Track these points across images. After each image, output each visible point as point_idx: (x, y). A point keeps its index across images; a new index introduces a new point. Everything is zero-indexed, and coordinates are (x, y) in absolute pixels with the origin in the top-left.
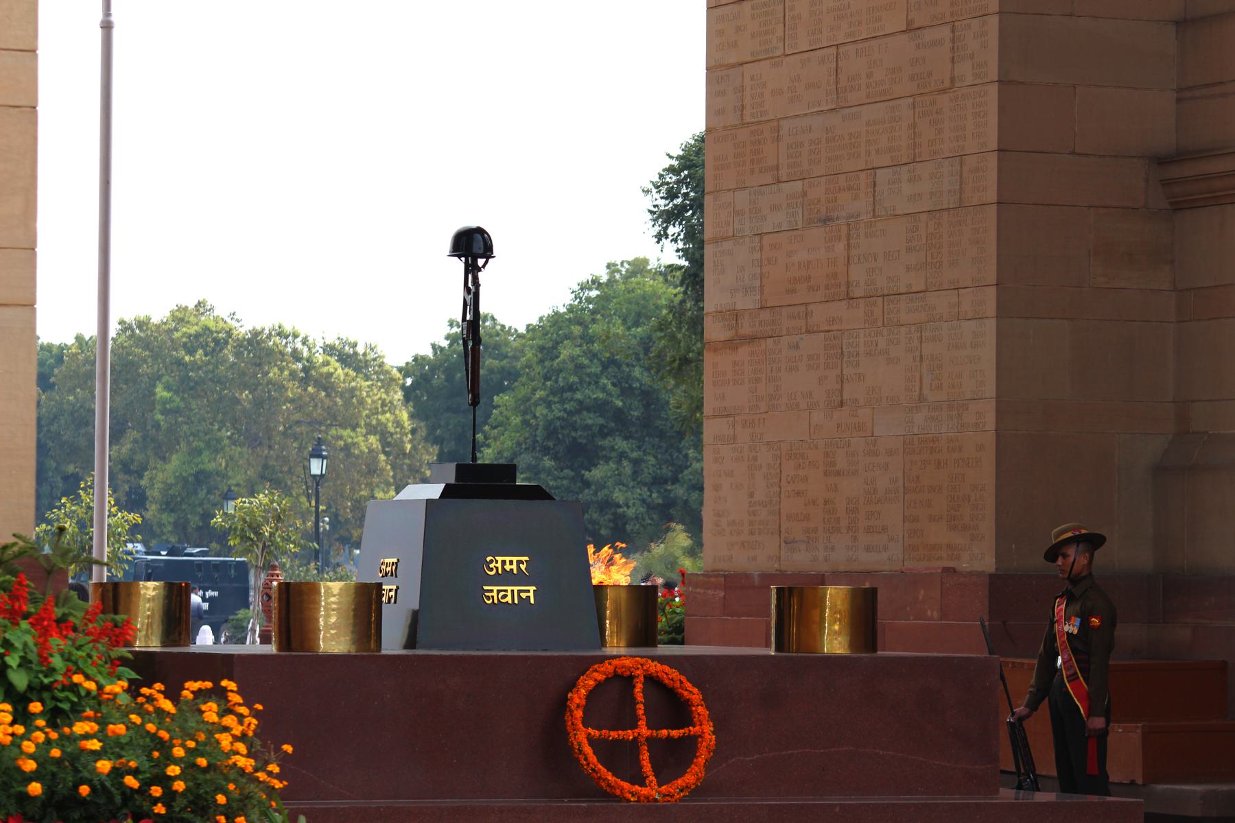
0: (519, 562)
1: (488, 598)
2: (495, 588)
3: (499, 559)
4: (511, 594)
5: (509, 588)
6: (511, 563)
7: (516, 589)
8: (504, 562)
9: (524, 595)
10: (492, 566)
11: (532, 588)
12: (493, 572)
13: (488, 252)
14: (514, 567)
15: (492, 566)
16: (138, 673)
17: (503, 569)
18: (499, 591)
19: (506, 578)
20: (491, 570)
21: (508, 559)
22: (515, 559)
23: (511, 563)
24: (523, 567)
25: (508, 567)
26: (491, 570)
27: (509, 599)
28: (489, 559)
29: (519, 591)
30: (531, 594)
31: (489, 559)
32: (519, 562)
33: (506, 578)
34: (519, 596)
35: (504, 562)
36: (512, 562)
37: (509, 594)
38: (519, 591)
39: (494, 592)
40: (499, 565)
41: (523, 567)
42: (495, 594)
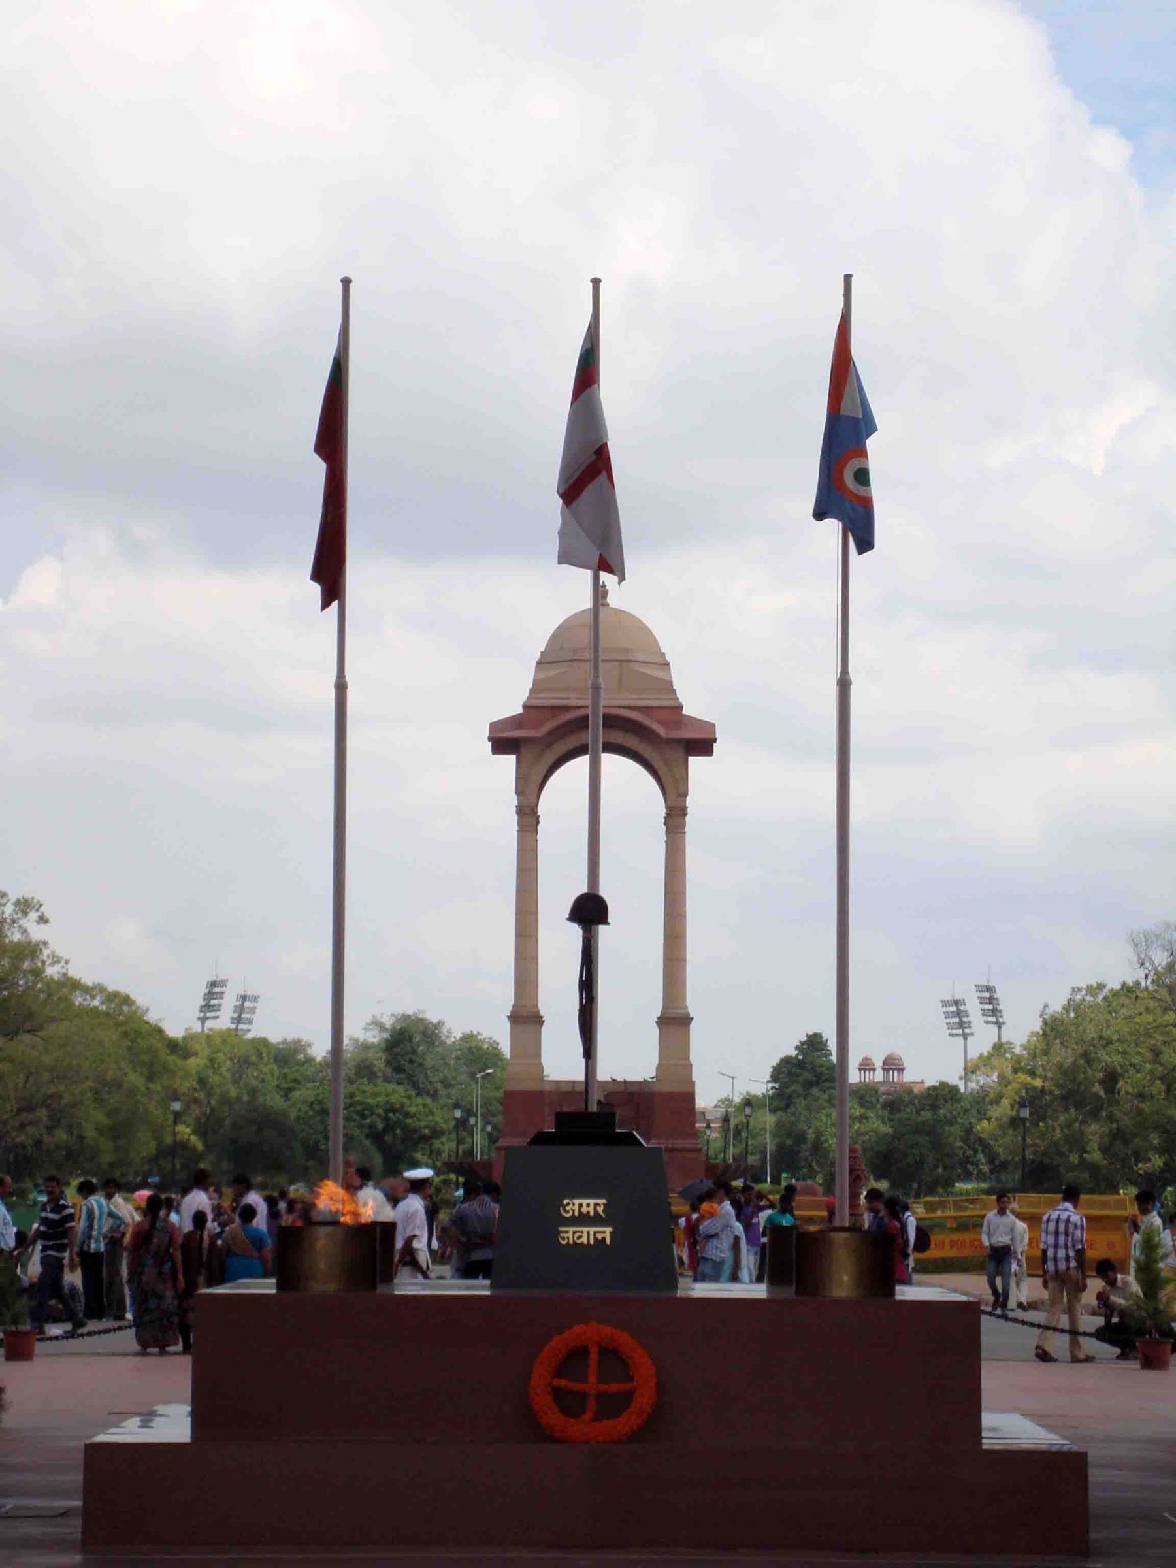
0: (596, 1205)
1: (563, 1239)
2: (571, 1229)
3: (577, 1202)
4: (587, 1234)
5: (585, 1229)
6: (588, 1205)
7: (592, 1230)
8: (581, 1205)
9: (599, 1236)
11: (608, 1230)
12: (571, 1213)
13: (1037, 1355)
18: (574, 1233)
19: (583, 1219)
21: (585, 1202)
22: (592, 1202)
23: (588, 1205)
25: (584, 1210)
27: (584, 1240)
28: (565, 1202)
29: (595, 1233)
31: (565, 1202)
33: (583, 1219)
34: (596, 1239)
35: (581, 1205)
36: (590, 1205)
37: (585, 1235)
38: (595, 1233)
39: (569, 1235)
40: (576, 1208)
41: (600, 1209)
42: (570, 1235)
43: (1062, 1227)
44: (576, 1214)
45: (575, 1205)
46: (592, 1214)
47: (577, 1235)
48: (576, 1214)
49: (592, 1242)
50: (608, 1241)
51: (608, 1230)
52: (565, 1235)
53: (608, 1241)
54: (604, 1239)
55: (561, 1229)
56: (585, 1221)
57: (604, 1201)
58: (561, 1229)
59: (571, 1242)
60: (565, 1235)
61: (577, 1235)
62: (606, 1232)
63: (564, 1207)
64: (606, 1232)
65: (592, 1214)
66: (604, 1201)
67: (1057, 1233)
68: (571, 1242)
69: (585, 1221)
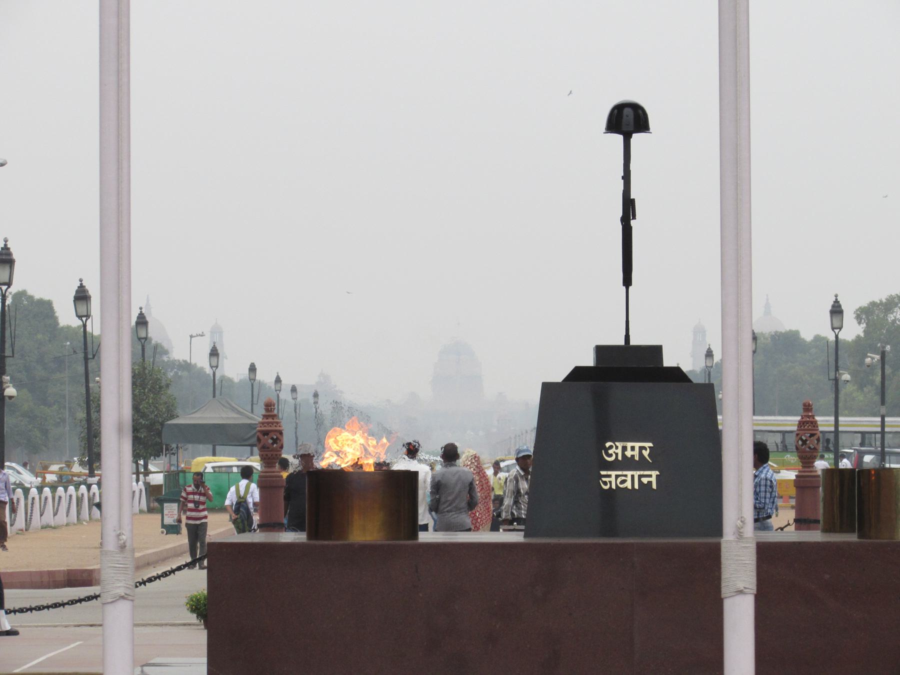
0: (641, 448)
1: (605, 483)
2: (613, 473)
4: (630, 479)
5: (629, 473)
6: (633, 448)
7: (637, 474)
8: (624, 449)
9: (645, 480)
10: (610, 452)
11: (655, 473)
14: (636, 453)
15: (610, 452)
16: (170, 425)
17: (624, 455)
18: (617, 477)
19: (627, 464)
20: (611, 455)
21: (629, 445)
22: (637, 445)
23: (633, 448)
24: (646, 453)
25: (629, 453)
26: (611, 455)
27: (628, 485)
28: (608, 444)
30: (653, 480)
32: (641, 448)
33: (627, 464)
34: (640, 482)
35: (624, 449)
36: (634, 449)
38: (640, 476)
39: (612, 479)
40: (619, 451)
41: (646, 453)
42: (613, 479)
43: (769, 483)
44: (620, 458)
45: (615, 450)
46: (637, 458)
47: (619, 480)
48: (620, 458)
49: (636, 487)
50: (654, 486)
51: (655, 473)
53: (654, 486)
54: (650, 483)
55: (603, 473)
57: (651, 445)
58: (603, 473)
59: (614, 487)
61: (619, 480)
62: (652, 477)
63: (606, 450)
64: (652, 477)
65: (637, 458)
66: (651, 445)
67: (766, 485)
68: (614, 487)
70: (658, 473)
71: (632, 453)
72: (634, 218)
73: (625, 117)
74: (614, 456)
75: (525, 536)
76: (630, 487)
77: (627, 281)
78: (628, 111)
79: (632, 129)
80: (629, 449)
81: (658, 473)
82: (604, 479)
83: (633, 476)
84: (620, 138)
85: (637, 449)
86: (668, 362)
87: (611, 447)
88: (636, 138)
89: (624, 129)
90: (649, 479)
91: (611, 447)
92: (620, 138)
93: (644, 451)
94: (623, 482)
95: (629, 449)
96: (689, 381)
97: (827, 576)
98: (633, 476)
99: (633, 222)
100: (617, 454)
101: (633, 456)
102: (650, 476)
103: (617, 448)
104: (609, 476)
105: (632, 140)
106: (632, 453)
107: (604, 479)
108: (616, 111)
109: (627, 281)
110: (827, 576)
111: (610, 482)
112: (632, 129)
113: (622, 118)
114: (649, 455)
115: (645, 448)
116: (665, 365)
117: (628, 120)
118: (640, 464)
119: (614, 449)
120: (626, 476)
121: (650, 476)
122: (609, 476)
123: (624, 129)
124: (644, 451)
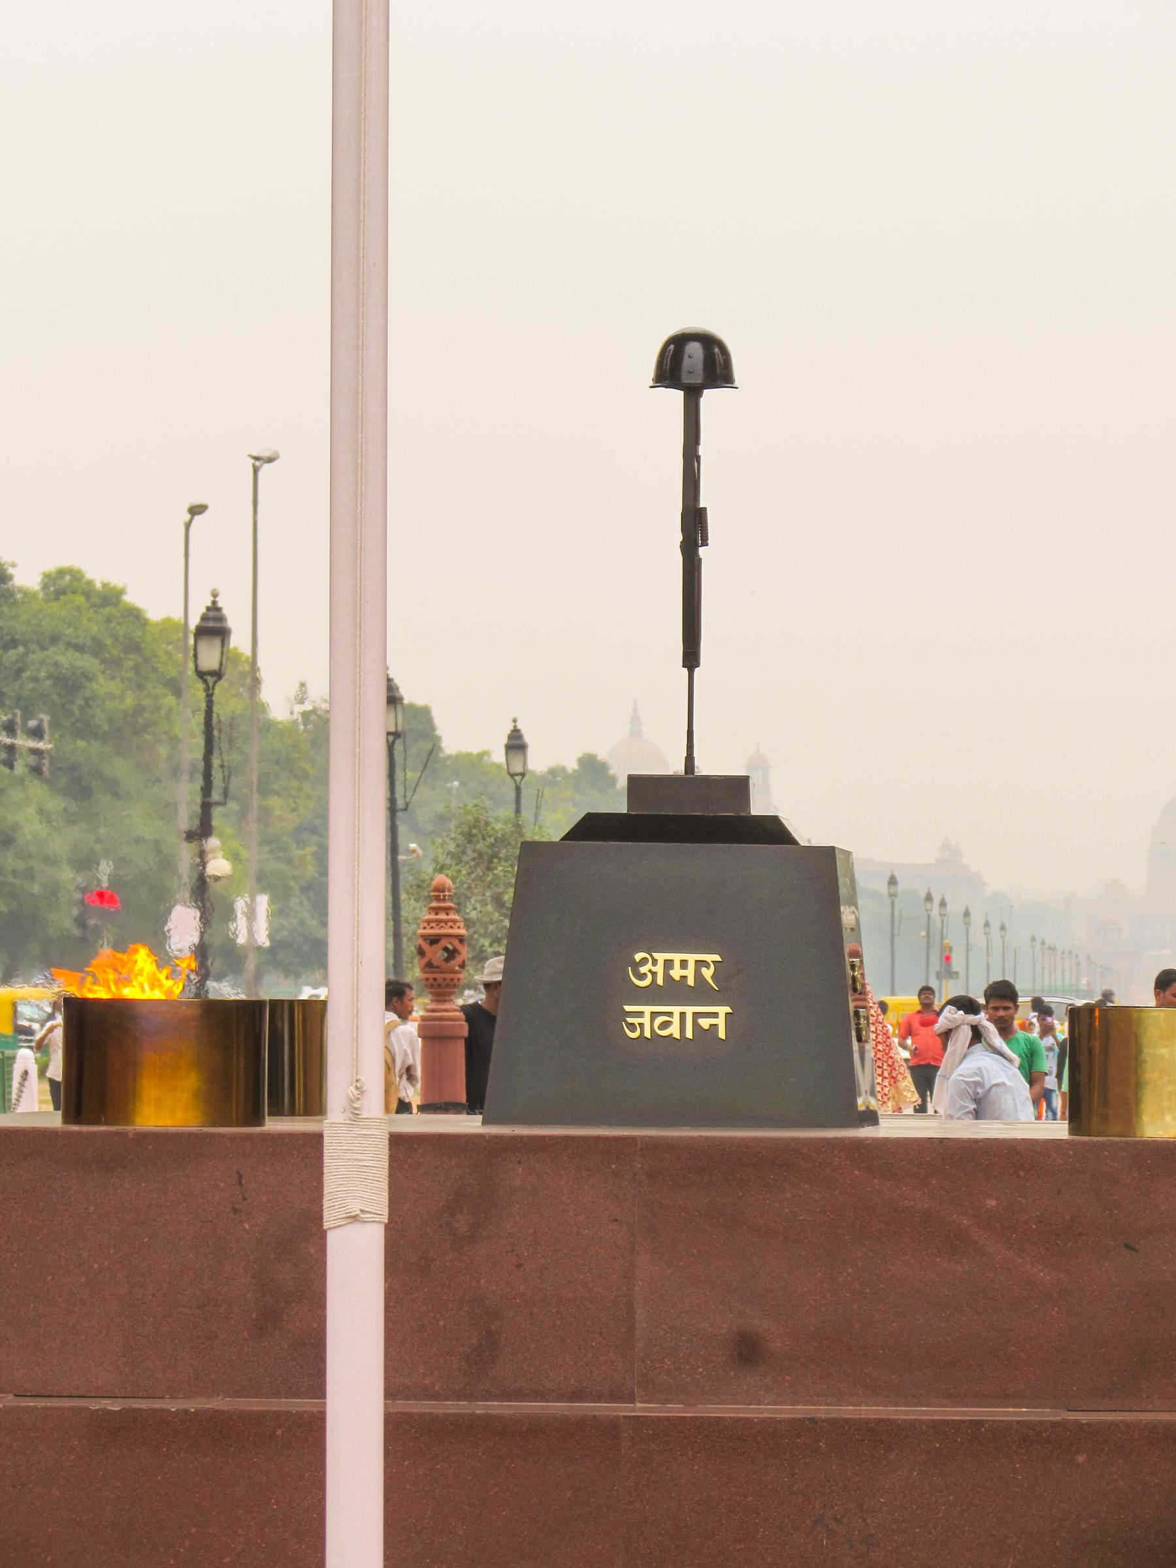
1: (632, 1027)
2: (648, 1010)
3: (661, 957)
4: (678, 1021)
5: (676, 1010)
6: (684, 965)
7: (690, 1010)
8: (669, 964)
9: (705, 1023)
10: (643, 970)
11: (723, 1010)
14: (690, 973)
15: (643, 970)
17: (667, 977)
18: (654, 1015)
19: (673, 992)
20: (642, 977)
21: (677, 957)
22: (692, 958)
23: (684, 965)
24: (708, 973)
25: (676, 973)
26: (642, 977)
27: (674, 1031)
28: (638, 957)
29: (696, 1015)
30: (721, 1022)
31: (638, 957)
33: (673, 992)
34: (695, 1023)
35: (669, 964)
36: (688, 965)
37: (676, 1020)
38: (696, 1015)
39: (644, 1020)
40: (659, 969)
41: (708, 973)
42: (646, 1020)
44: (660, 981)
45: (654, 965)
46: (691, 982)
48: (660, 981)
49: (689, 1034)
50: (722, 1034)
52: (636, 1021)
53: (722, 1034)
55: (628, 1008)
56: (675, 995)
57: (717, 958)
58: (628, 1008)
59: (648, 1034)
60: (636, 1021)
62: (718, 1017)
63: (636, 966)
64: (718, 1017)
65: (691, 982)
66: (717, 958)
68: (648, 1034)
69: (675, 995)
70: (728, 1010)
71: (684, 973)
72: (705, 543)
73: (686, 363)
74: (649, 975)
75: (484, 1123)
76: (677, 1035)
77: (691, 658)
78: (695, 350)
79: (698, 379)
80: (677, 964)
81: (728, 1010)
82: (630, 1020)
83: (683, 1015)
84: (678, 396)
85: (691, 966)
86: (758, 808)
87: (644, 961)
88: (710, 398)
89: (686, 379)
90: (713, 1021)
91: (644, 961)
92: (678, 396)
93: (704, 970)
94: (665, 1025)
95: (677, 964)
96: (793, 842)
97: (991, 1203)
98: (683, 1015)
99: (702, 551)
100: (654, 974)
101: (684, 978)
102: (715, 1015)
103: (655, 962)
104: (640, 1014)
105: (702, 400)
106: (684, 973)
107: (630, 1020)
108: (672, 347)
109: (691, 658)
110: (991, 1203)
111: (641, 1025)
112: (698, 379)
113: (682, 359)
114: (713, 977)
115: (704, 964)
116: (753, 813)
117: (694, 365)
118: (699, 993)
119: (649, 966)
120: (670, 1014)
121: (715, 1015)
122: (640, 1014)
123: (686, 379)
124: (704, 970)
